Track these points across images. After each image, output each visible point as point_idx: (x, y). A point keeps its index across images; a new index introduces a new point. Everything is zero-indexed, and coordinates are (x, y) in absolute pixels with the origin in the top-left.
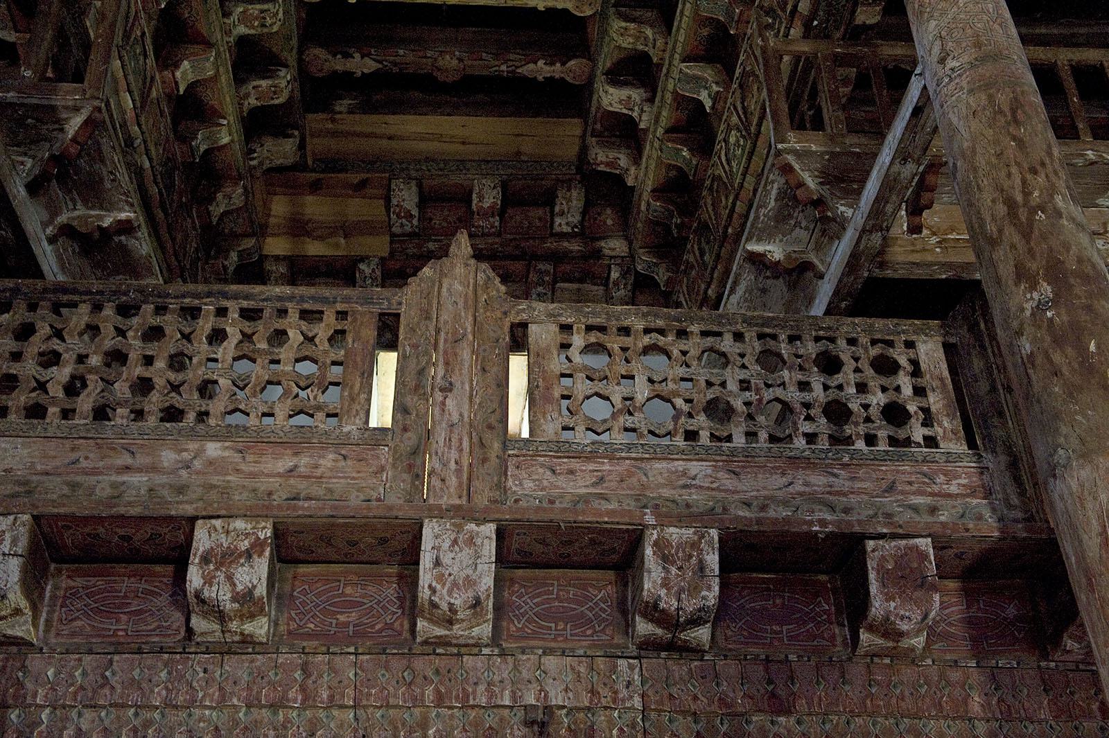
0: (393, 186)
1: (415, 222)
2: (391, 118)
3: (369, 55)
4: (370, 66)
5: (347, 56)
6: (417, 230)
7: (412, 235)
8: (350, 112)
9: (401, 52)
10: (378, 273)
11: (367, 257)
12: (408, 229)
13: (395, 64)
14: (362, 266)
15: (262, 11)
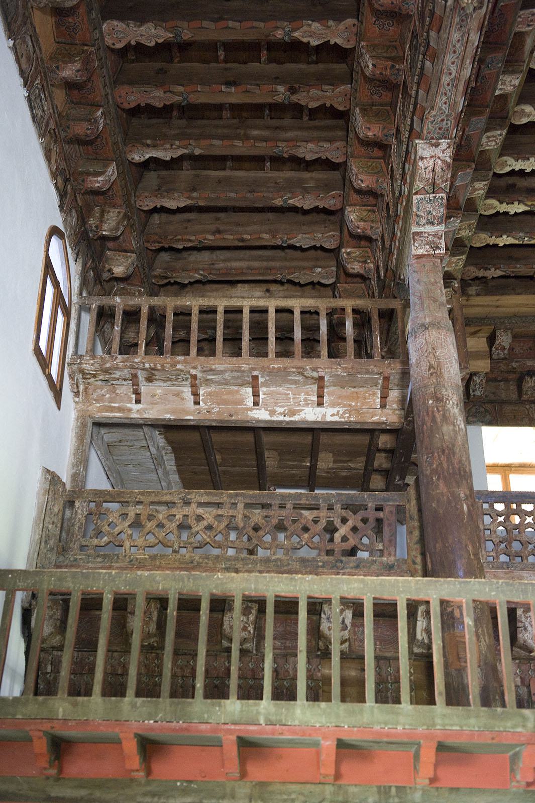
0: (497, 334)
1: (506, 352)
2: (503, 298)
3: (498, 268)
4: (499, 273)
5: (486, 269)
6: (507, 357)
7: (505, 359)
8: (478, 295)
9: (518, 266)
10: (484, 382)
11: (478, 373)
12: (502, 356)
13: (513, 272)
14: (475, 378)
15: (459, 259)
